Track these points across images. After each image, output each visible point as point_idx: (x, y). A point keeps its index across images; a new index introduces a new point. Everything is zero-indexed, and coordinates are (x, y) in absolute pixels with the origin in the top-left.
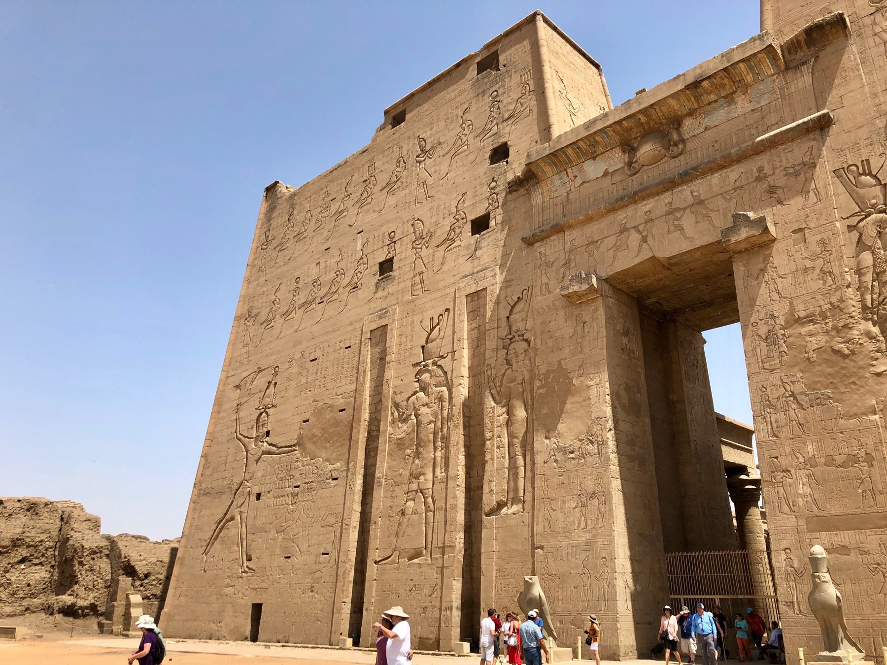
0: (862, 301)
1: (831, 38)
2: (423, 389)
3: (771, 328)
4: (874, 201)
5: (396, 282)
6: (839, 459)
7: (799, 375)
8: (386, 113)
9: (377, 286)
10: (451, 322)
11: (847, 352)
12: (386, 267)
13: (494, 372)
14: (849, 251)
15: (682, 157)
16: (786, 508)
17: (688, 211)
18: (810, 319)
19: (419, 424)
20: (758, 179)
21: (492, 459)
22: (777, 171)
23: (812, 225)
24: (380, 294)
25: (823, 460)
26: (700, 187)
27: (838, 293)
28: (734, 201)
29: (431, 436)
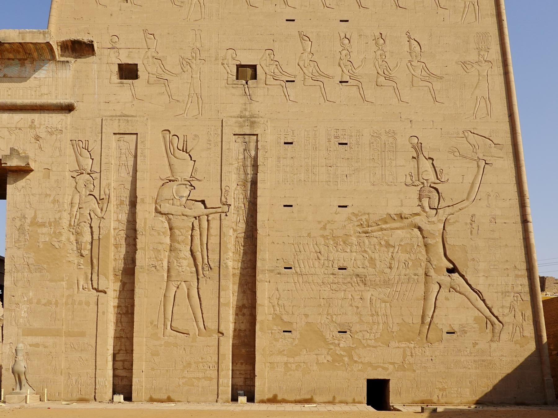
0: (70, 221)
1: (85, 52)
3: (22, 223)
4: (86, 167)
6: (44, 301)
7: (33, 254)
11: (57, 247)
16: (14, 323)
18: (43, 225)
20: (31, 127)
22: (42, 127)
23: (54, 169)
25: (36, 301)
27: (59, 214)
28: (14, 136)
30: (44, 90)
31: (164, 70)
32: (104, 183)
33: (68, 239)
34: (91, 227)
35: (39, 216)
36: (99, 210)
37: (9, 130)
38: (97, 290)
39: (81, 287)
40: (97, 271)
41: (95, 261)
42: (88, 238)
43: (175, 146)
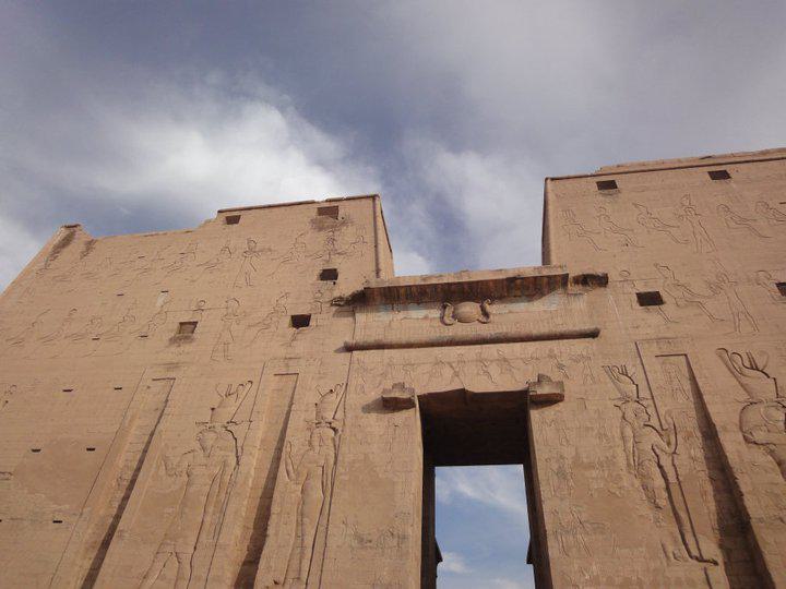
2: (204, 449)
5: (194, 344)
6: (618, 580)
8: (219, 212)
9: (173, 341)
10: (253, 392)
12: (187, 329)
13: (295, 450)
14: (617, 423)
15: (490, 325)
17: (494, 364)
18: (591, 466)
19: (189, 484)
21: (276, 534)
24: (173, 349)
25: (605, 579)
26: (505, 348)
29: (204, 499)
30: (559, 321)
31: (692, 294)
32: (662, 411)
33: (633, 485)
34: (660, 467)
35: (584, 455)
36: (664, 445)
37: (525, 361)
38: (700, 559)
39: (671, 555)
40: (690, 530)
41: (683, 515)
42: (659, 482)
43: (740, 363)
